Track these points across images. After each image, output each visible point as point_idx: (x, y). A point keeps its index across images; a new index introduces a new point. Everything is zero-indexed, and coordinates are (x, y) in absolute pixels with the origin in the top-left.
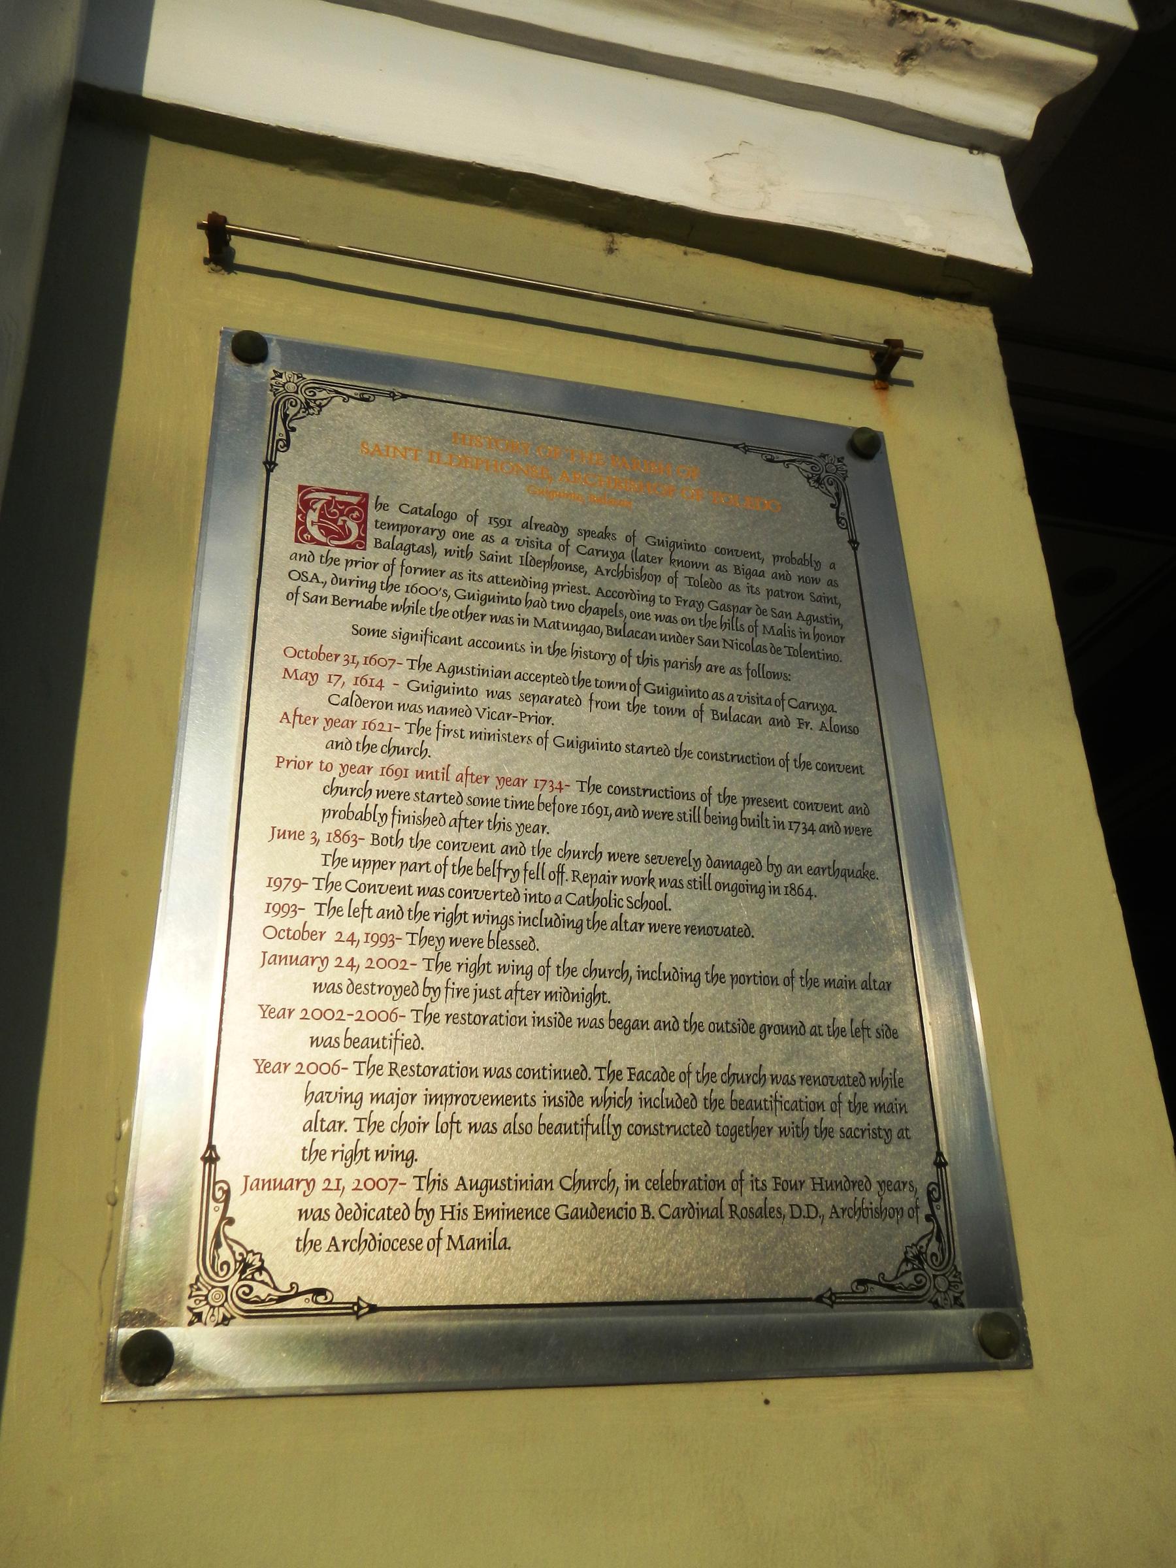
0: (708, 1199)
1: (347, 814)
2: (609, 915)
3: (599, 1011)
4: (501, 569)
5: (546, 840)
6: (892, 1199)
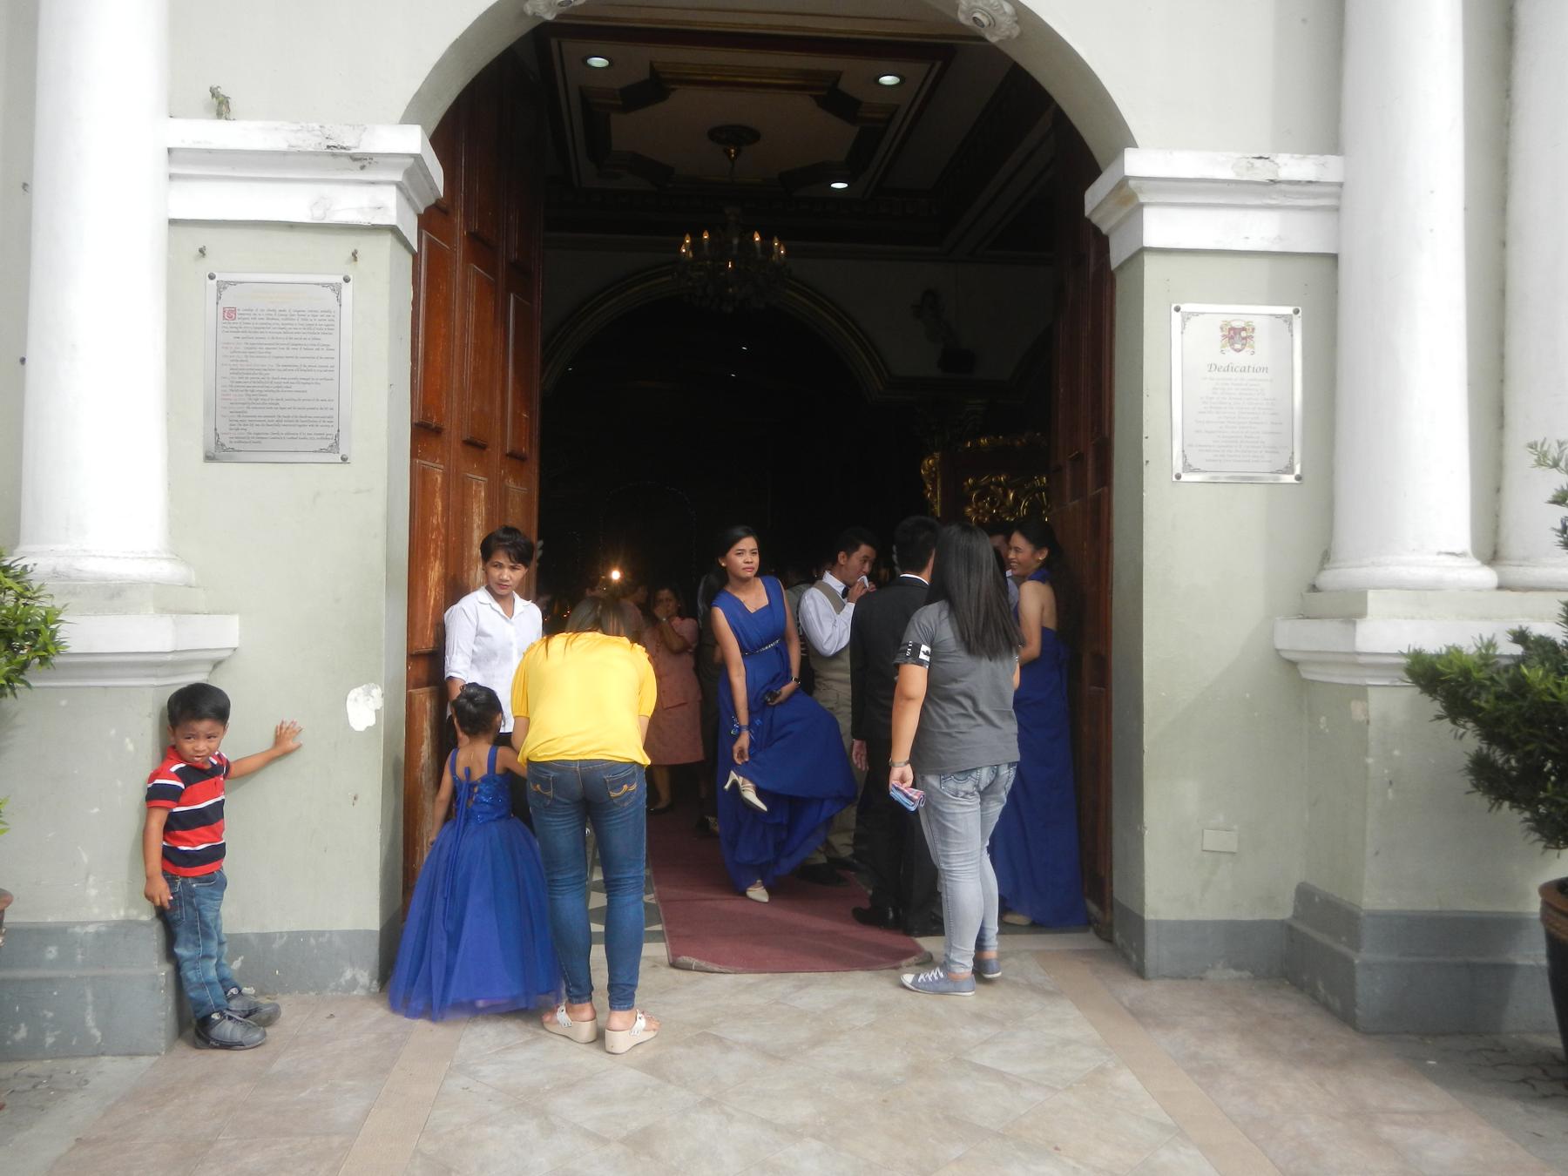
0: (295, 436)
1: (233, 373)
2: (280, 389)
3: (278, 406)
4: (262, 321)
5: (270, 376)
6: (329, 436)
